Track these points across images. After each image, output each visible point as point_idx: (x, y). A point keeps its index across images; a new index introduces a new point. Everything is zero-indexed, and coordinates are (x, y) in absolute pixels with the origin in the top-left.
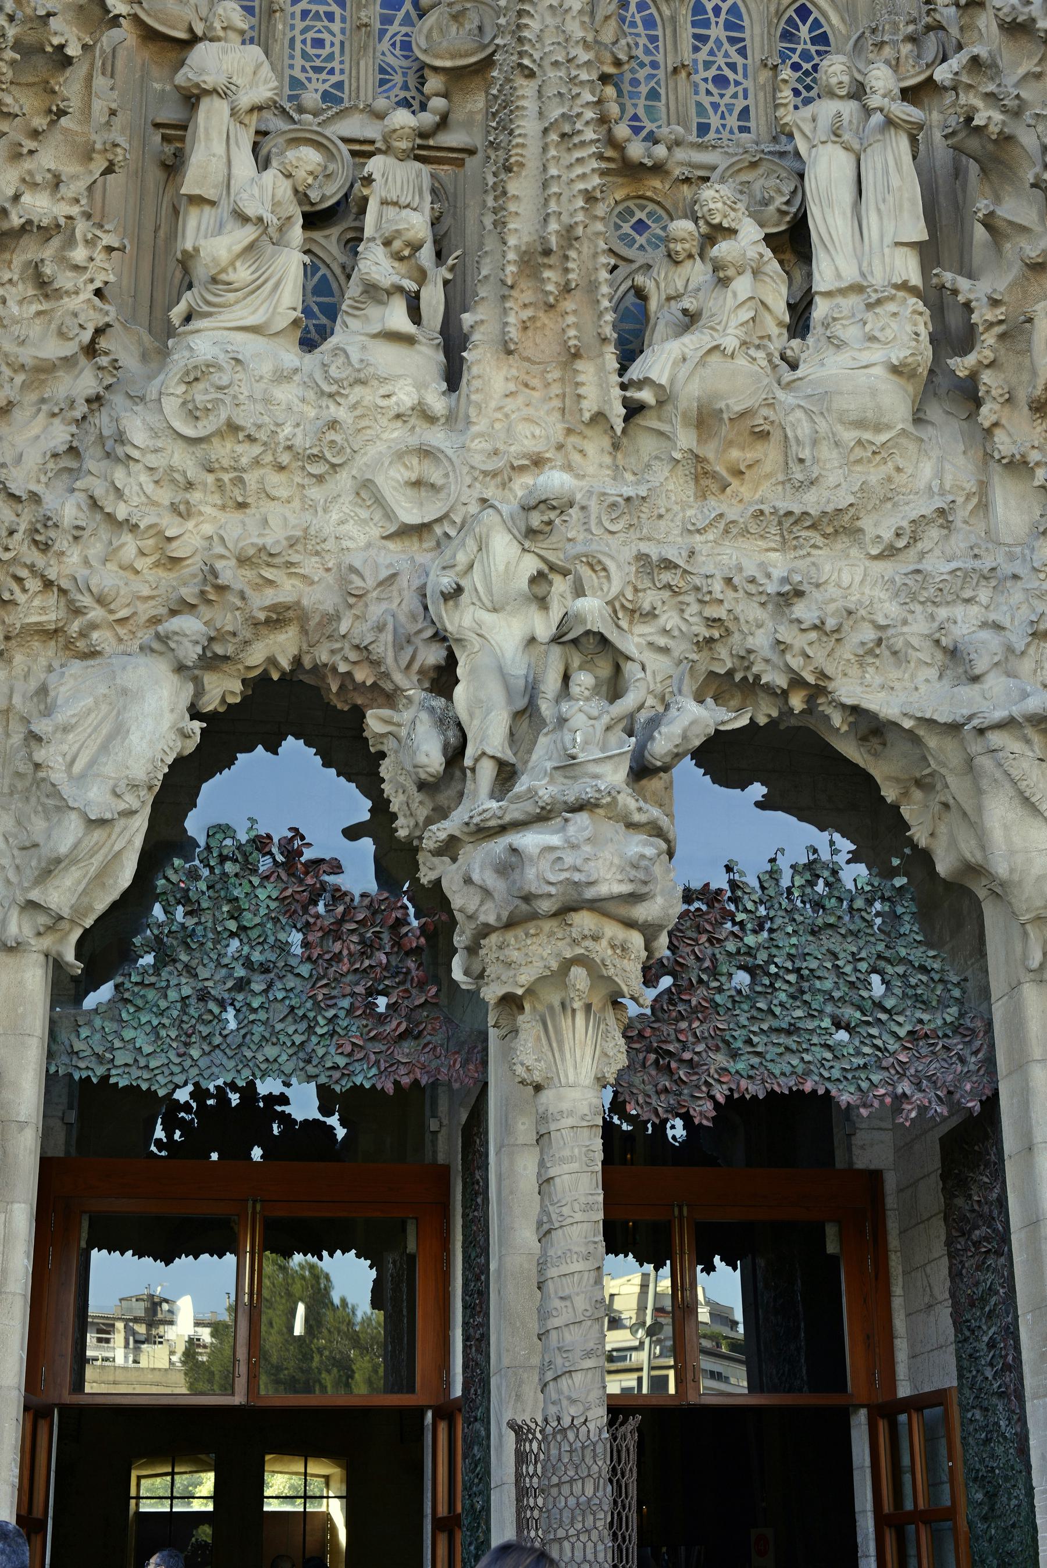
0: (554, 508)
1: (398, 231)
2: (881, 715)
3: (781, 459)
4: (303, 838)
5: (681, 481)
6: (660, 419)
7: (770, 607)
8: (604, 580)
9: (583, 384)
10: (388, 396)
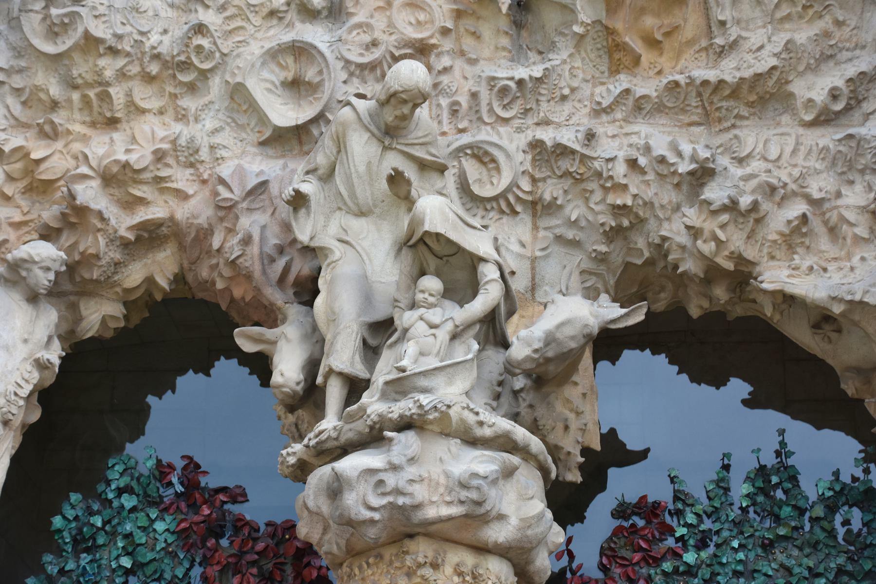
0: (405, 102)
2: (808, 301)
3: (702, 22)
4: (198, 466)
5: (592, 56)
7: (685, 187)
8: (494, 173)
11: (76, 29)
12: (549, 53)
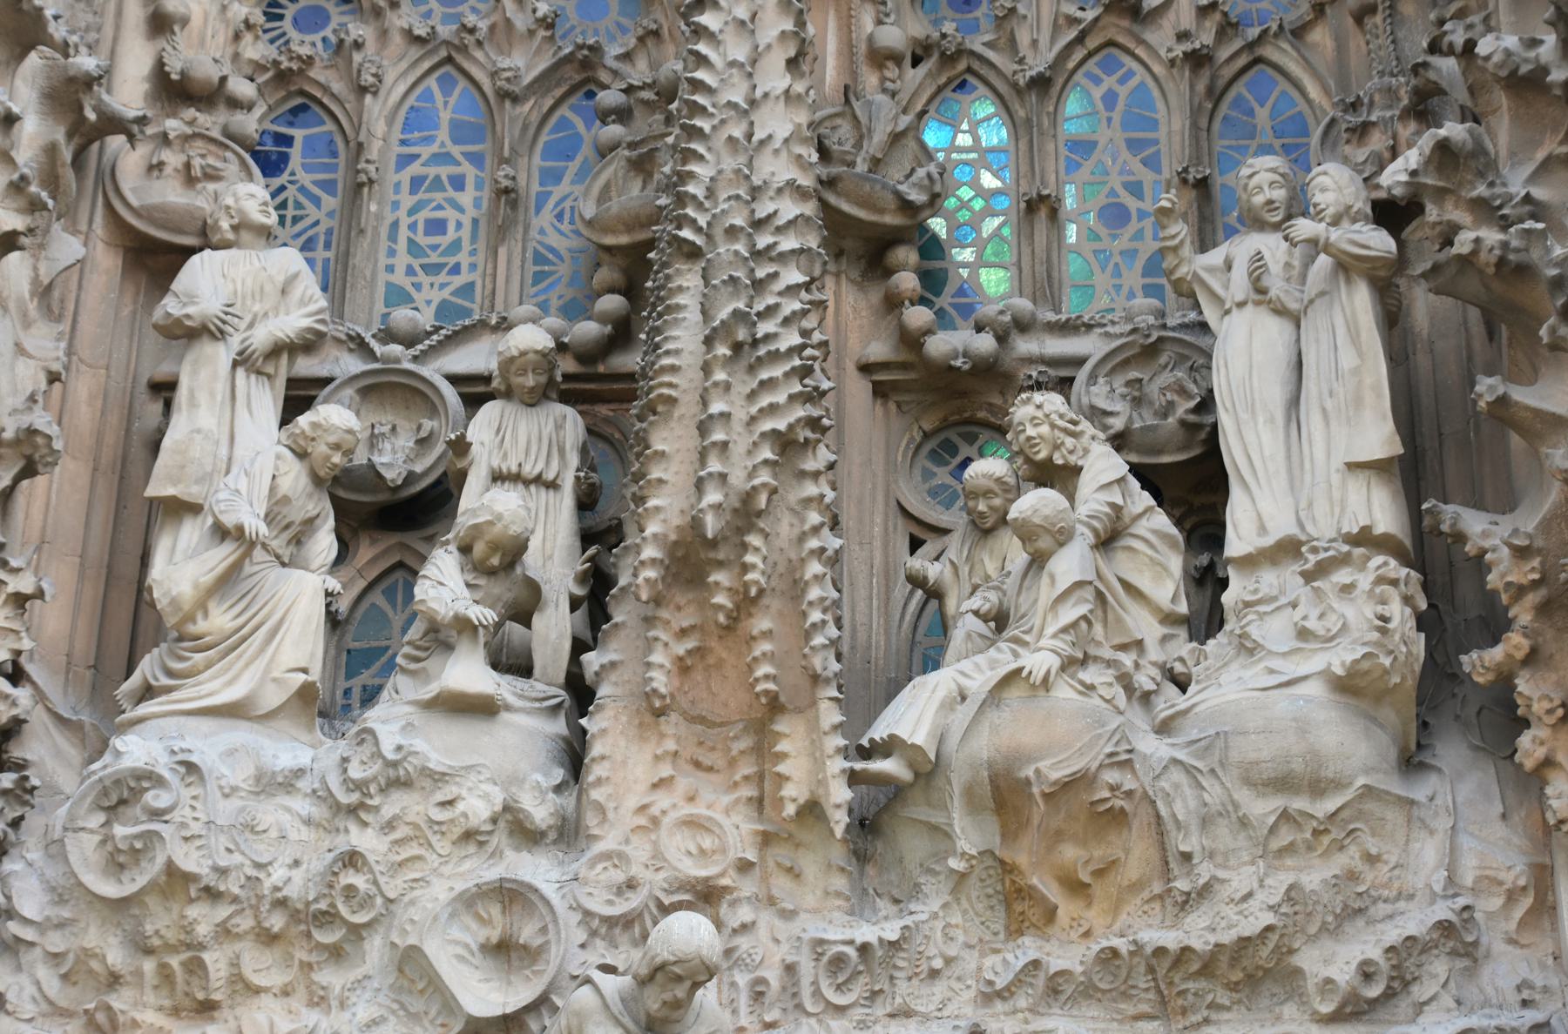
0: (679, 979)
1: (476, 526)
3: (1154, 854)
5: (980, 907)
6: (929, 804)
9: (782, 756)
10: (450, 803)
11: (152, 859)
12: (909, 901)
